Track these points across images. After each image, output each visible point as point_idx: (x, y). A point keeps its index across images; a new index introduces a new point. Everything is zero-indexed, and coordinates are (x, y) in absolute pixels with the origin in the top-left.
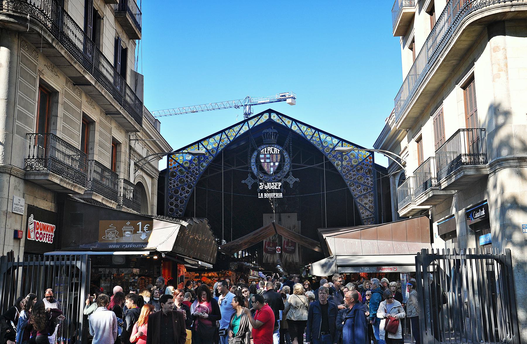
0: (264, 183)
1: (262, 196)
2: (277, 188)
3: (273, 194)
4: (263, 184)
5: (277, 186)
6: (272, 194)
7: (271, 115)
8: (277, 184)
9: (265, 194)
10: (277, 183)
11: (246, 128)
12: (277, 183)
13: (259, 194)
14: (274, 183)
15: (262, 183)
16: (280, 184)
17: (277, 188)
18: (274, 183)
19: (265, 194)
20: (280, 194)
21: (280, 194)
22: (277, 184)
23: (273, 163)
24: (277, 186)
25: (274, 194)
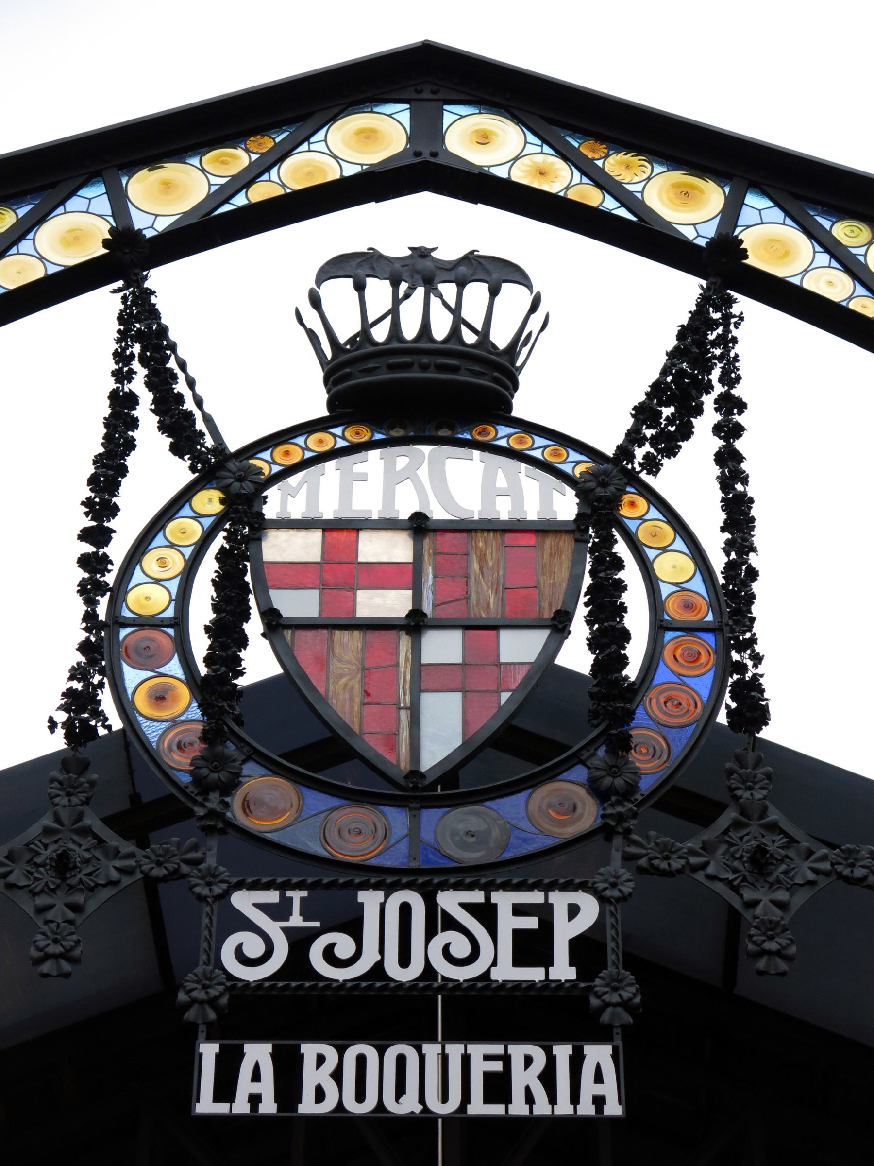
0: (297, 896)
1: (267, 1088)
2: (535, 974)
3: (455, 1050)
4: (279, 912)
5: (517, 934)
6: (432, 1050)
7: (448, 118)
8: (519, 910)
9: (309, 1050)
10: (536, 897)
11: (74, 237)
12: (536, 897)
13: (209, 1051)
14: (477, 897)
15: (272, 897)
16: (573, 911)
17: (535, 974)
18: (477, 897)
19: (309, 1050)
20: (577, 1061)
21: (577, 1061)
22: (519, 910)
23: (456, 637)
24: (517, 934)
25: (477, 1050)
